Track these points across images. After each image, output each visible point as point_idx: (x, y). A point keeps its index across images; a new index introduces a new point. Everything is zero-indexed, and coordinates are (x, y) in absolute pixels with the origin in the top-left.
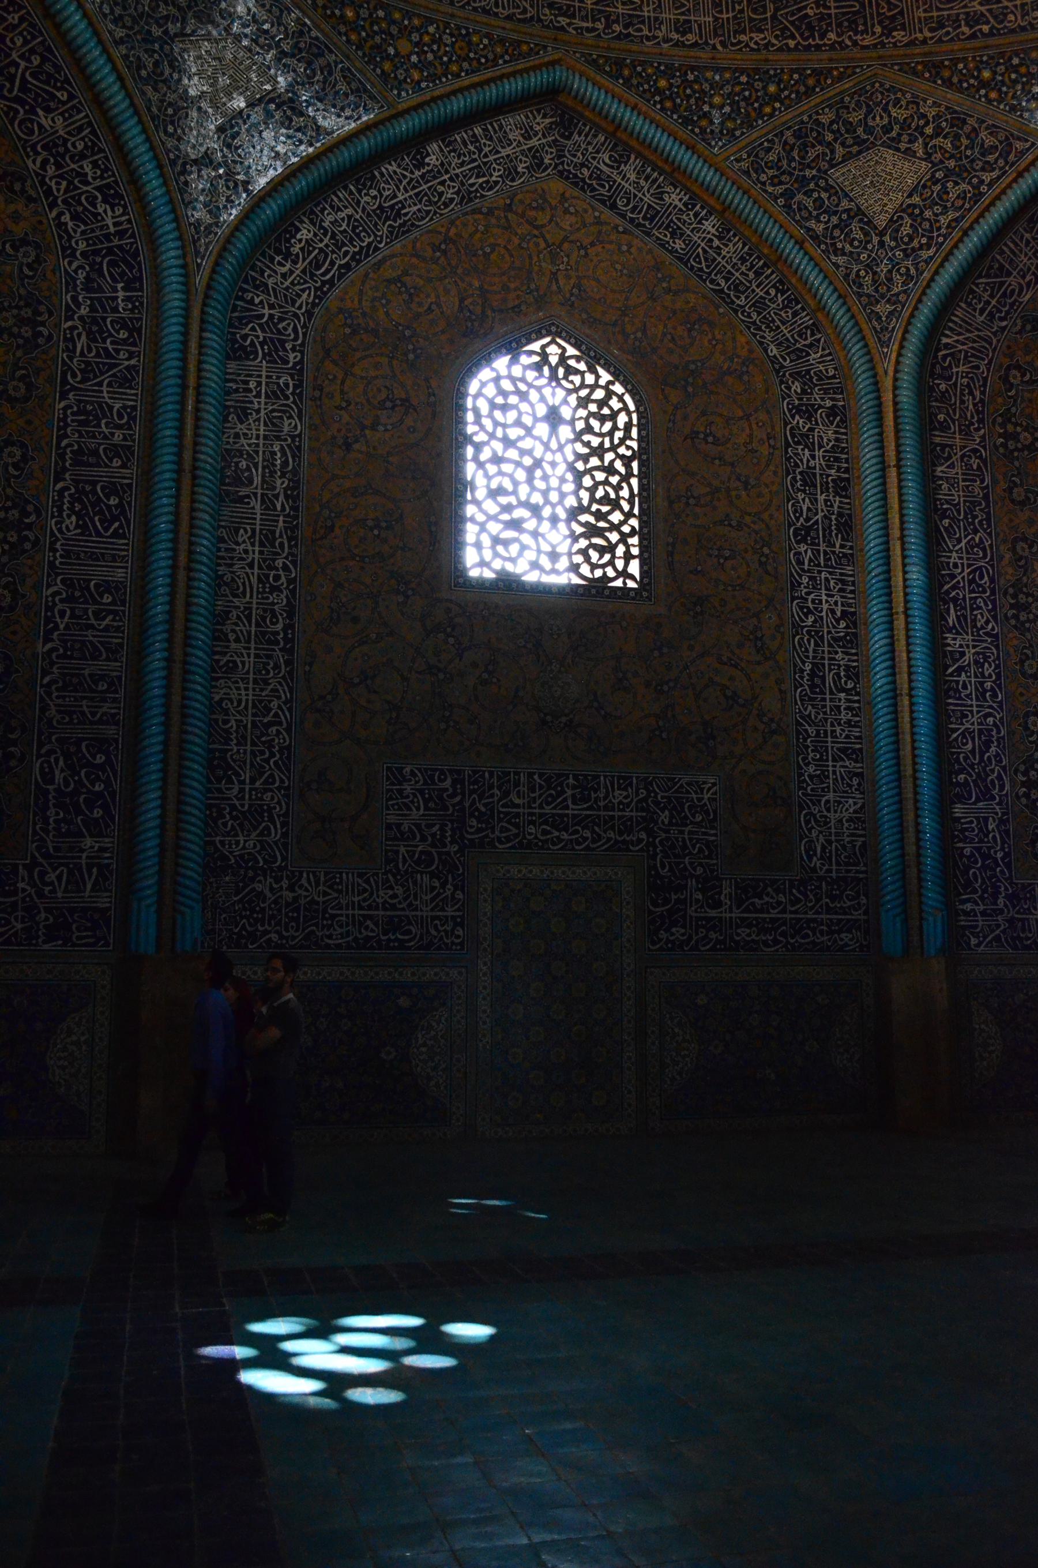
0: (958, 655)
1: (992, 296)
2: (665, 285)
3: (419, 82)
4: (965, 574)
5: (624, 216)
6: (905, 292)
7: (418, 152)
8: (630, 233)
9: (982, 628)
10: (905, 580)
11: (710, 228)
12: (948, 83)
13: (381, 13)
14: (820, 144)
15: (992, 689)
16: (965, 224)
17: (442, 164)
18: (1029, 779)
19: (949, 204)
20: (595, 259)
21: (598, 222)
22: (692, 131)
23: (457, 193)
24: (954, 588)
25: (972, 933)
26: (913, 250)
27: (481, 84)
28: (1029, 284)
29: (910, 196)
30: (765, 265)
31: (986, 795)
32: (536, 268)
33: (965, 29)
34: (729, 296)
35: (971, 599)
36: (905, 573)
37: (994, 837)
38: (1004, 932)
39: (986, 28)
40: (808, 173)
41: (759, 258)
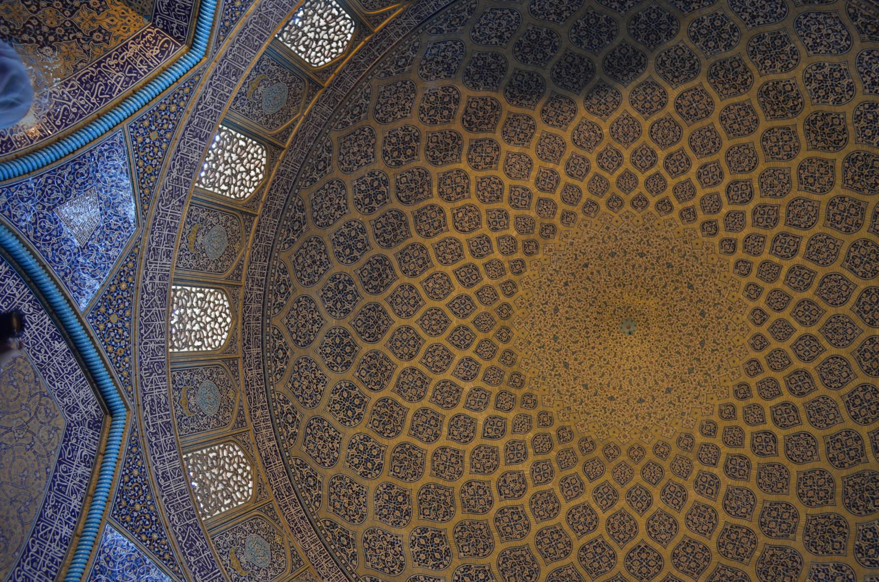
2: (23, 508)
3: (98, 329)
5: (56, 471)
7: (59, 337)
8: (47, 477)
11: (64, 531)
13: (127, 304)
14: (138, 577)
17: (56, 351)
20: (26, 456)
21: (49, 454)
22: (117, 497)
23: (43, 362)
27: (106, 366)
30: (54, 577)
32: (11, 417)
34: (27, 557)
41: (56, 571)
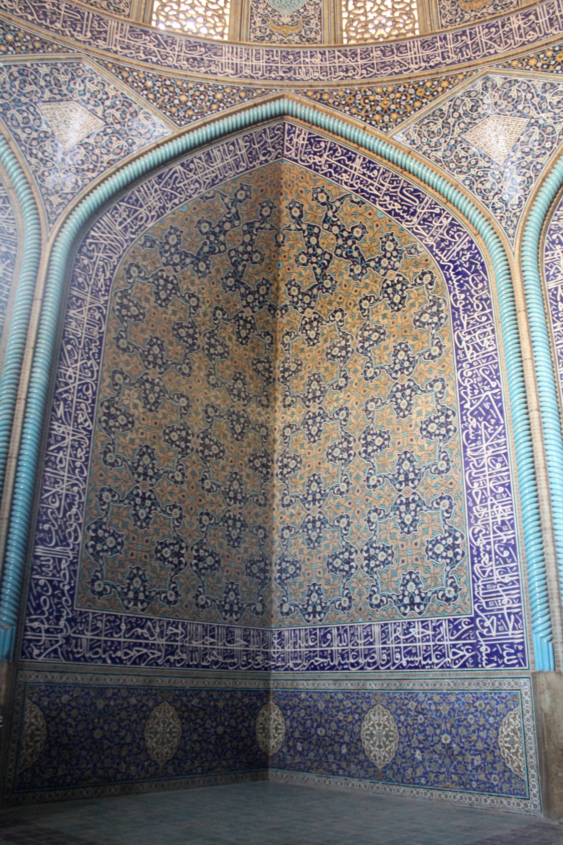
0: (59, 438)
1: (128, 216)
4: (76, 384)
6: (72, 194)
9: (81, 424)
10: (31, 377)
12: (126, 80)
14: (36, 84)
15: (81, 467)
16: (119, 164)
18: (97, 536)
19: (111, 150)
24: (66, 392)
25: (36, 646)
26: (83, 170)
28: (153, 217)
29: (88, 137)
31: (64, 542)
33: (142, 54)
35: (77, 402)
36: (32, 372)
37: (64, 574)
38: (61, 646)
39: (154, 59)
40: (23, 99)
